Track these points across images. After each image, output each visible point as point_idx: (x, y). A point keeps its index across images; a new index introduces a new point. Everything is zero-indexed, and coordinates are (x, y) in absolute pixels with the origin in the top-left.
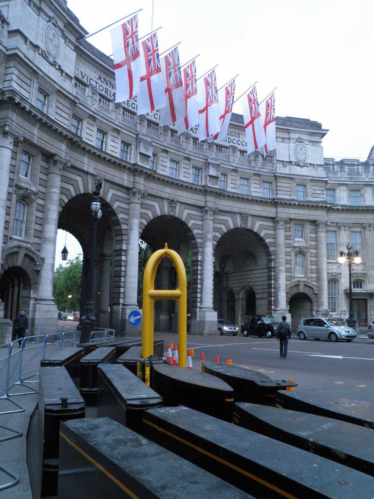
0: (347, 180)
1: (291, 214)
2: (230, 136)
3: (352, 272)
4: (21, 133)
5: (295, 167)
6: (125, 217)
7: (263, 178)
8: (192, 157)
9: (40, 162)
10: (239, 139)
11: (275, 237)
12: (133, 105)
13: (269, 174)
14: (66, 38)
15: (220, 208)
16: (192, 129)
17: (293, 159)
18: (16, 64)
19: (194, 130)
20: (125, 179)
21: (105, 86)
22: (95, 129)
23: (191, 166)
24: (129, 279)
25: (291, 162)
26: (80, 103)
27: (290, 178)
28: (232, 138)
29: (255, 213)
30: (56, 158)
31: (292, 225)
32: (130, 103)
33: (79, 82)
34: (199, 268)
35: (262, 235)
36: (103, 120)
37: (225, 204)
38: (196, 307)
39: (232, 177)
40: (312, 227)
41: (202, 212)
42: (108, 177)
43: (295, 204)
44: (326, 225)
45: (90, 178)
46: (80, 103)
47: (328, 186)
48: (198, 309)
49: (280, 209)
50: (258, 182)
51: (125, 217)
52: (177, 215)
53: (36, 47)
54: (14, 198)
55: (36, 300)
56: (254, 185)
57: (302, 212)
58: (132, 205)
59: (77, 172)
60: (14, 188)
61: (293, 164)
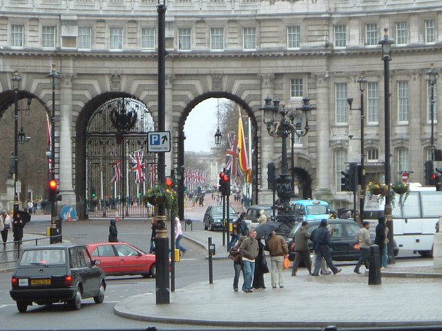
0: (360, 9)
1: (278, 67)
3: (365, 138)
7: (245, 24)
8: (139, 19)
13: (249, 18)
15: (177, 73)
20: (49, 66)
22: (9, 28)
23: (139, 28)
24: (62, 166)
27: (275, 19)
35: (243, 98)
36: (15, 16)
39: (199, 31)
40: (311, 81)
42: (29, 69)
43: (279, 55)
44: (326, 79)
47: (335, 22)
49: (264, 63)
50: (236, 30)
56: (229, 36)
57: (293, 63)
58: (62, 90)
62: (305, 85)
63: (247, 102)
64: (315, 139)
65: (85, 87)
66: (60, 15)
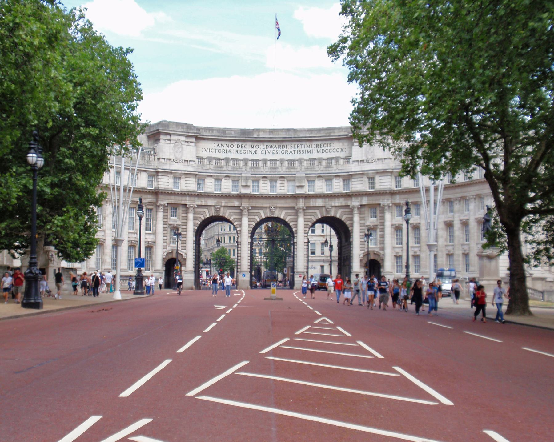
4: (166, 202)
5: (367, 163)
6: (239, 223)
11: (352, 219)
12: (244, 152)
14: (188, 142)
16: (291, 152)
17: (364, 158)
18: (160, 174)
19: (293, 152)
25: (363, 161)
28: (325, 149)
29: (337, 204)
30: (187, 206)
31: (365, 209)
32: (242, 151)
35: (343, 219)
37: (312, 203)
40: (381, 209)
45: (213, 208)
51: (239, 223)
52: (276, 216)
53: (170, 159)
54: (169, 229)
55: (185, 271)
59: (206, 207)
60: (168, 225)
61: (365, 161)
62: (378, 212)
63: (345, 222)
64: (382, 243)
65: (255, 214)
66: (241, 174)
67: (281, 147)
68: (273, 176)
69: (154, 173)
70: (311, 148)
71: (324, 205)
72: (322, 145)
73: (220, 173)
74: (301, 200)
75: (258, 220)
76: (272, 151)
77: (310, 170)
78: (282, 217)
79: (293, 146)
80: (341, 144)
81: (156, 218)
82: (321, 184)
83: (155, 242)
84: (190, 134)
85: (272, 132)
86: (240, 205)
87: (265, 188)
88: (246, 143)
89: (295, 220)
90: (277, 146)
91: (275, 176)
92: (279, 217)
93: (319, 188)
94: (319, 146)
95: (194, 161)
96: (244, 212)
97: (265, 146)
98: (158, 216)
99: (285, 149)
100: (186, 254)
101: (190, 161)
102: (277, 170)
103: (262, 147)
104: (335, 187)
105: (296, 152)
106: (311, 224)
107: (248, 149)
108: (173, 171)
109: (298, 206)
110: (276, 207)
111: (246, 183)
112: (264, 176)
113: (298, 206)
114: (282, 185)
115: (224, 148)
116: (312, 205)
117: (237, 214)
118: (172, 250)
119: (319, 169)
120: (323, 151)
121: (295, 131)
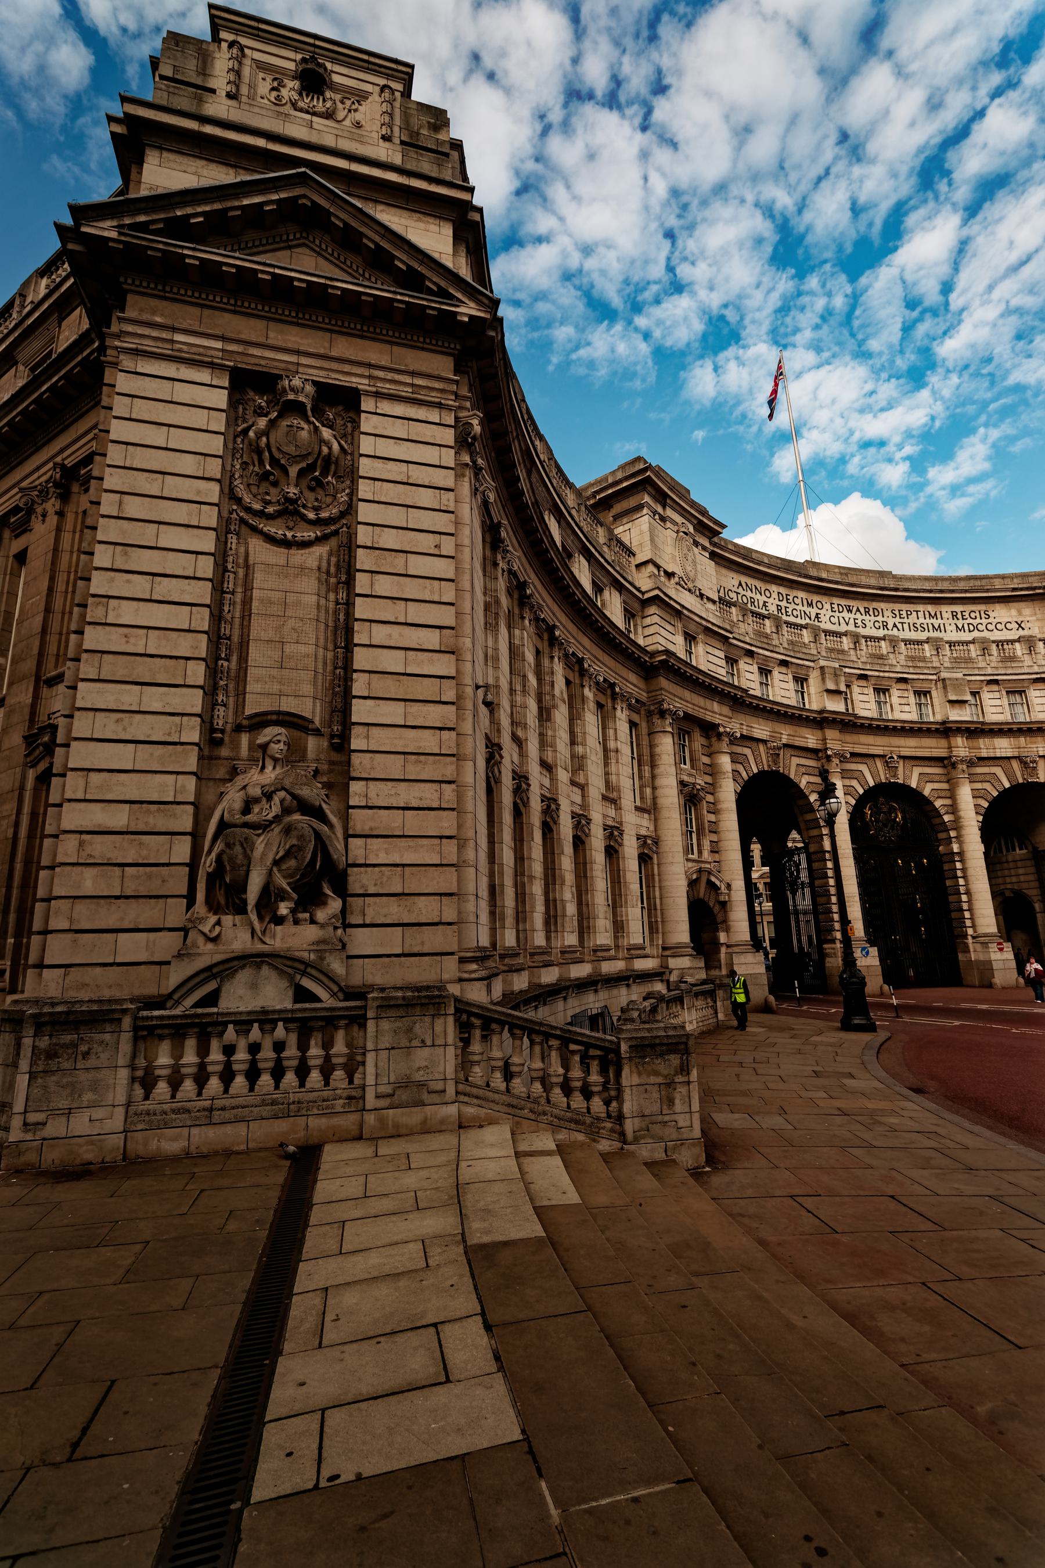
2: (970, 621)
9: (698, 741)
10: (989, 621)
16: (895, 625)
19: (900, 626)
21: (749, 594)
26: (734, 638)
30: (721, 729)
33: (724, 602)
34: (958, 865)
38: (966, 936)
41: (945, 767)
45: (762, 747)
46: (734, 638)
48: (970, 940)
52: (901, 781)
55: (728, 946)
67: (871, 613)
68: (882, 674)
69: (637, 606)
70: (940, 621)
71: (1016, 754)
72: (967, 614)
73: (772, 651)
74: (959, 741)
75: (861, 791)
76: (852, 621)
77: (963, 665)
78: (914, 785)
79: (897, 612)
80: (1014, 612)
81: (653, 756)
82: (998, 702)
83: (656, 842)
84: (705, 520)
85: (846, 574)
86: (819, 747)
87: (867, 706)
88: (795, 593)
89: (943, 794)
90: (862, 610)
91: (886, 675)
92: (907, 782)
93: (994, 710)
94: (959, 616)
95: (714, 602)
96: (834, 764)
97: (835, 606)
98: (658, 750)
99: (880, 618)
100: (729, 886)
101: (708, 599)
102: (886, 662)
103: (827, 606)
104: (1038, 708)
105: (906, 626)
106: (986, 805)
107: (799, 607)
108: (685, 612)
109: (954, 753)
110: (900, 757)
111: (837, 684)
112: (862, 672)
113: (954, 753)
114: (903, 701)
115: (753, 595)
116: (984, 754)
117: (811, 771)
118: (700, 871)
119: (991, 665)
120: (972, 628)
121: (895, 577)
